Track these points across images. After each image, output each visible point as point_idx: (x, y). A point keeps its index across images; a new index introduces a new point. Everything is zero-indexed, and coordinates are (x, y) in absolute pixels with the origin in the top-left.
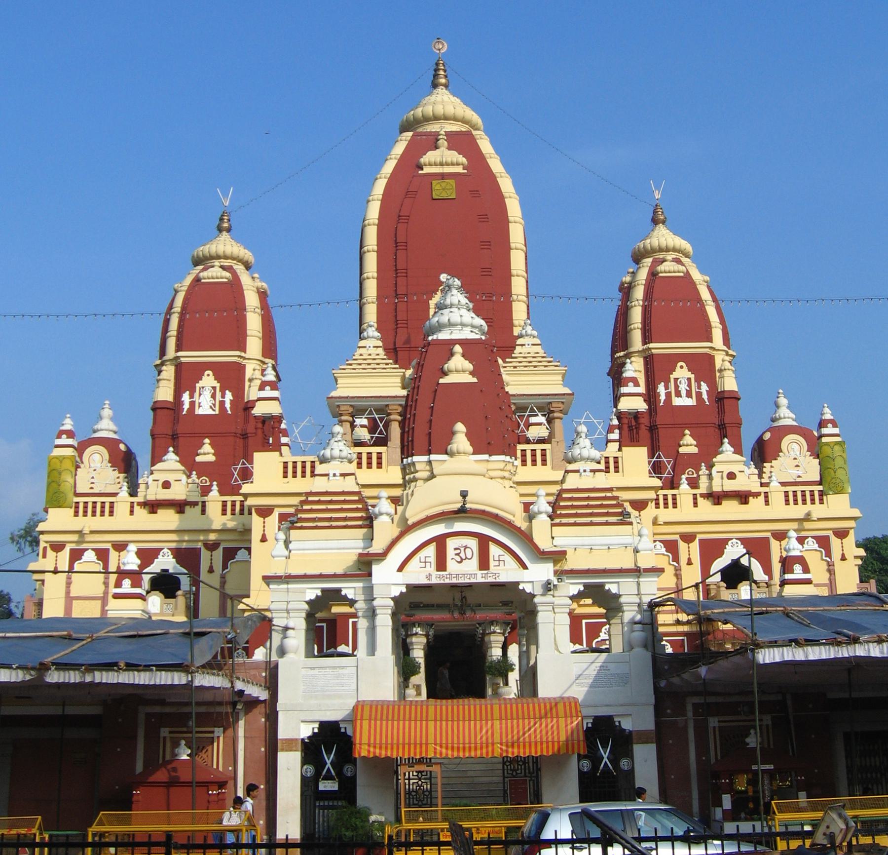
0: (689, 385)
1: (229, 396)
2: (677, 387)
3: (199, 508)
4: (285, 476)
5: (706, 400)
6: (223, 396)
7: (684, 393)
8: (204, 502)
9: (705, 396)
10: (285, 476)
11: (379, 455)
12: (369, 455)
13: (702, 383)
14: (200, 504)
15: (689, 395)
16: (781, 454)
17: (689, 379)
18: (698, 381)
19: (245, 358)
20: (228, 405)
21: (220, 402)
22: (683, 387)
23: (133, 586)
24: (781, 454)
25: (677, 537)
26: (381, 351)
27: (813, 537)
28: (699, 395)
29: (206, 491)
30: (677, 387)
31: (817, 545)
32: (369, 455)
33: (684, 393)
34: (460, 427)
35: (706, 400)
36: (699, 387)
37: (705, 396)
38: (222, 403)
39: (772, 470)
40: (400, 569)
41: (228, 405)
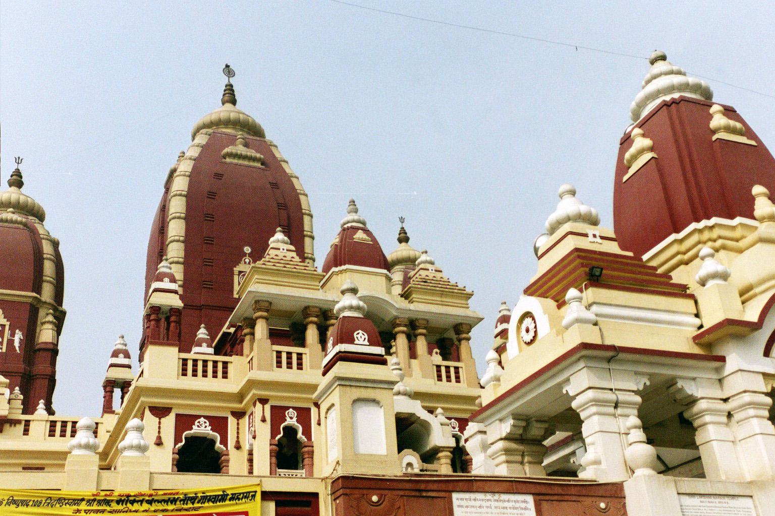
1: (18, 336)
3: (21, 428)
6: (13, 335)
8: (27, 423)
10: (184, 374)
11: (300, 356)
12: (289, 354)
14: (23, 423)
19: (39, 301)
20: (17, 344)
21: (9, 340)
23: (372, 343)
26: (294, 254)
29: (29, 408)
32: (289, 354)
34: (757, 189)
38: (11, 342)
40: (767, 353)
41: (17, 344)
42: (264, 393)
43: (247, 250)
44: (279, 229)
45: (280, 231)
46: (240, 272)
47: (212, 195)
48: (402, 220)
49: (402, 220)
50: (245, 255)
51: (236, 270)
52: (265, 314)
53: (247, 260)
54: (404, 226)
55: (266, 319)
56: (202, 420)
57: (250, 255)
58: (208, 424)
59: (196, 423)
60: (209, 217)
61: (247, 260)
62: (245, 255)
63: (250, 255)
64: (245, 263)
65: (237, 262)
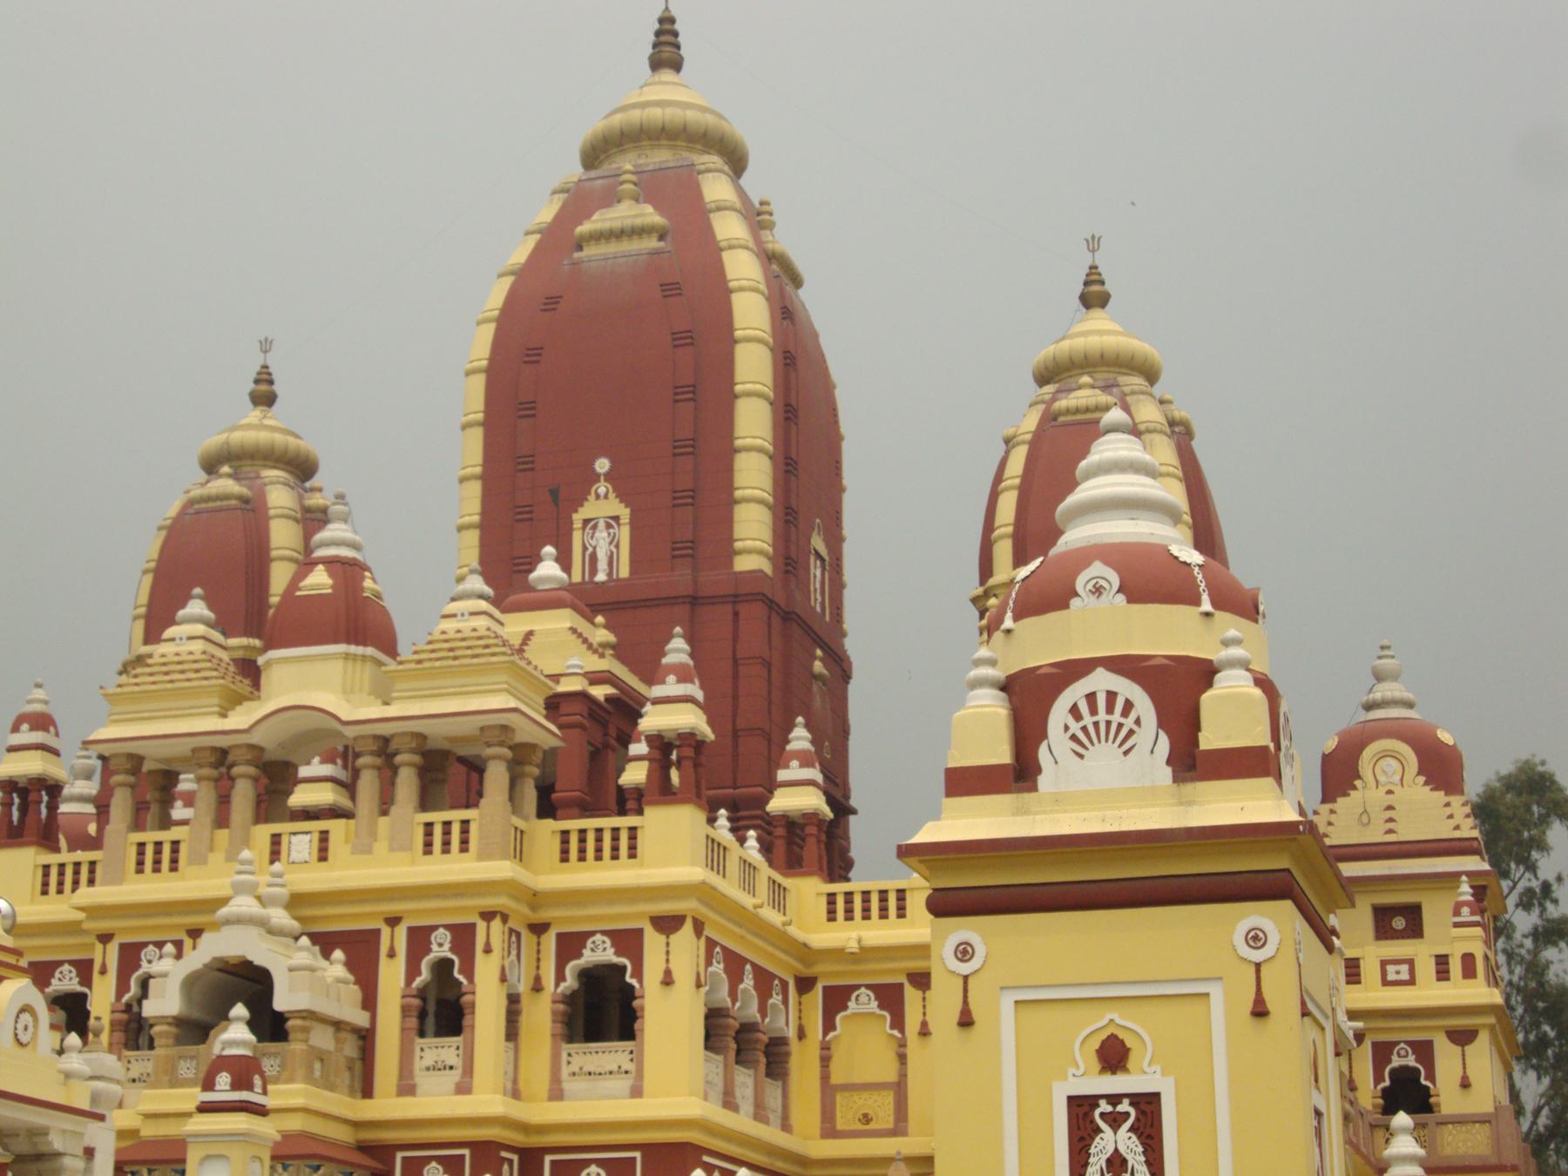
4: (45, 892)
10: (45, 892)
16: (1358, 783)
24: (1358, 783)
25: (903, 979)
27: (868, 987)
31: (874, 1004)
39: (1333, 818)
42: (105, 925)
43: (602, 465)
44: (198, 591)
45: (201, 598)
46: (586, 522)
47: (534, 354)
48: (1093, 244)
49: (1093, 244)
50: (596, 478)
51: (578, 518)
52: (132, 779)
53: (602, 490)
54: (1097, 263)
55: (132, 787)
56: (66, 967)
57: (609, 477)
58: (74, 974)
59: (57, 975)
60: (527, 409)
61: (602, 490)
62: (596, 478)
63: (609, 477)
64: (598, 497)
65: (580, 501)
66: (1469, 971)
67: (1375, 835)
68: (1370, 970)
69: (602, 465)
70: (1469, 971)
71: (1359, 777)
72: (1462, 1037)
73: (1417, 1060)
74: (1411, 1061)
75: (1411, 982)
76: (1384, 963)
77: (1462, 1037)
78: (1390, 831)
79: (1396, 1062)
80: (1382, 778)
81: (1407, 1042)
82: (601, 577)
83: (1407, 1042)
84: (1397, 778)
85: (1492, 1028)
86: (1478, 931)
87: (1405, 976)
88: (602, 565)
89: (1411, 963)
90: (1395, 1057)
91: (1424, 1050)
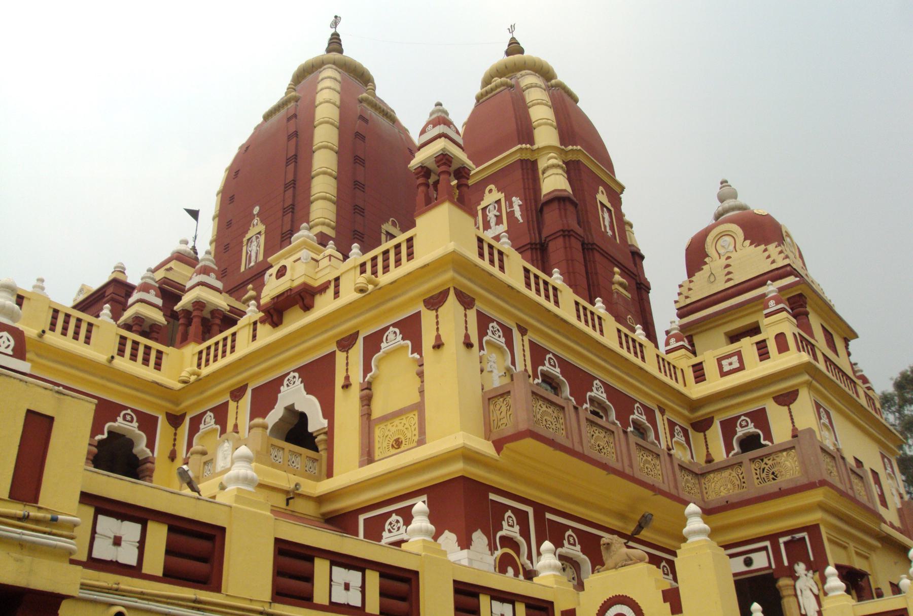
0: (500, 210)
2: (485, 216)
5: (520, 218)
7: (493, 221)
9: (518, 214)
13: (514, 199)
15: (499, 220)
17: (498, 202)
18: (508, 199)
22: (492, 215)
28: (511, 215)
30: (485, 216)
33: (493, 221)
35: (520, 218)
36: (511, 206)
37: (518, 214)
39: (692, 285)
57: (258, 215)
66: (783, 346)
67: (721, 286)
68: (711, 369)
69: (256, 210)
70: (783, 346)
71: (707, 256)
72: (787, 399)
73: (755, 427)
74: (751, 429)
75: (742, 368)
76: (719, 360)
77: (787, 399)
78: (729, 280)
79: (740, 432)
80: (721, 251)
81: (745, 415)
82: (252, 264)
83: (745, 415)
84: (731, 248)
85: (809, 385)
86: (784, 314)
87: (736, 365)
88: (253, 258)
89: (739, 354)
90: (738, 429)
91: (760, 417)
